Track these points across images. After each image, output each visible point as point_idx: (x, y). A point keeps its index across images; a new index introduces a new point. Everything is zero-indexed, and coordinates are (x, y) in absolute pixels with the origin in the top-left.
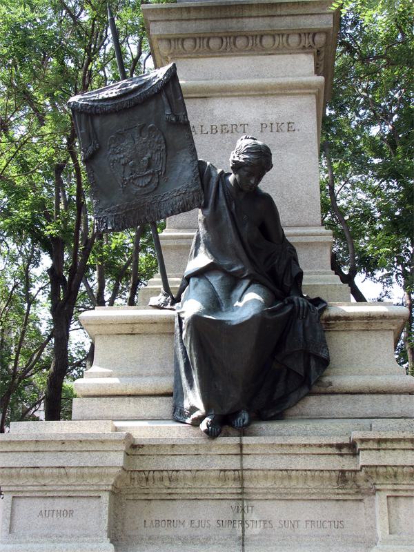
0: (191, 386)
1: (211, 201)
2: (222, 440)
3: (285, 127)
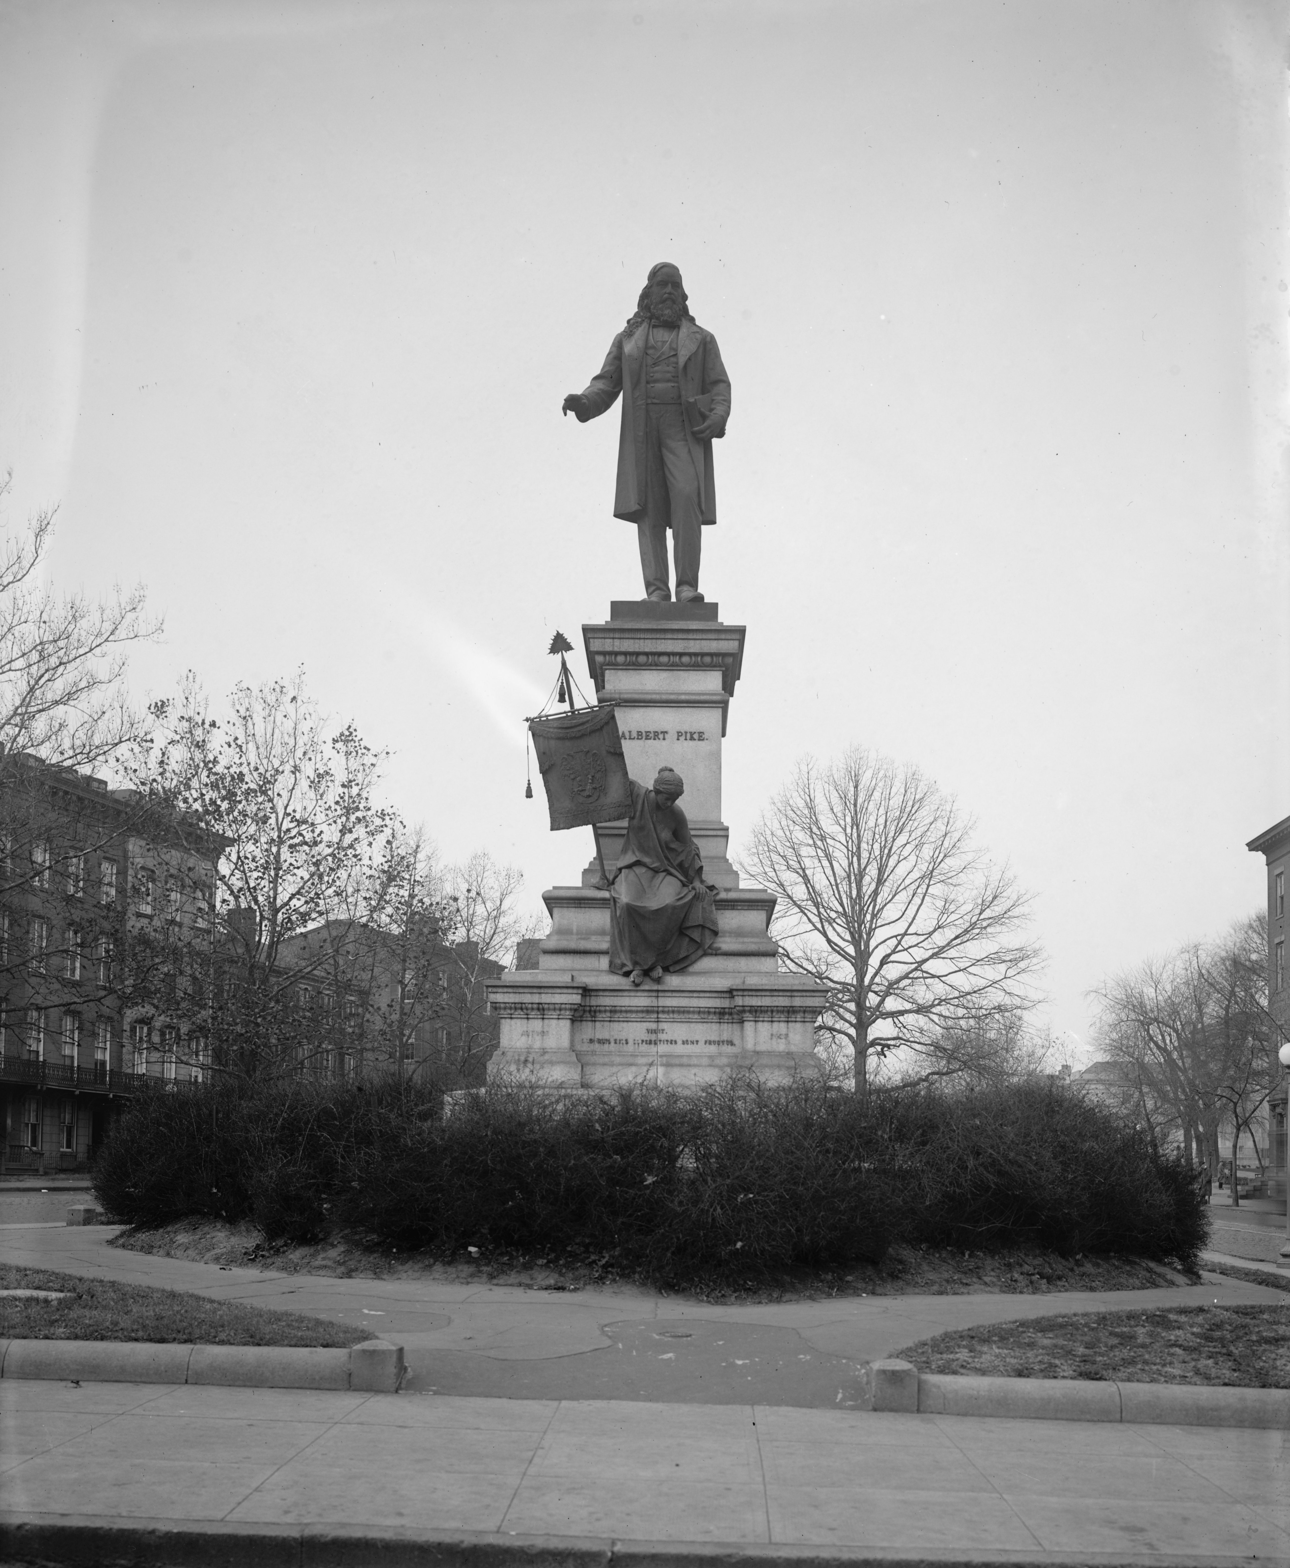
0: (623, 949)
1: (638, 814)
2: (642, 988)
3: (696, 736)
